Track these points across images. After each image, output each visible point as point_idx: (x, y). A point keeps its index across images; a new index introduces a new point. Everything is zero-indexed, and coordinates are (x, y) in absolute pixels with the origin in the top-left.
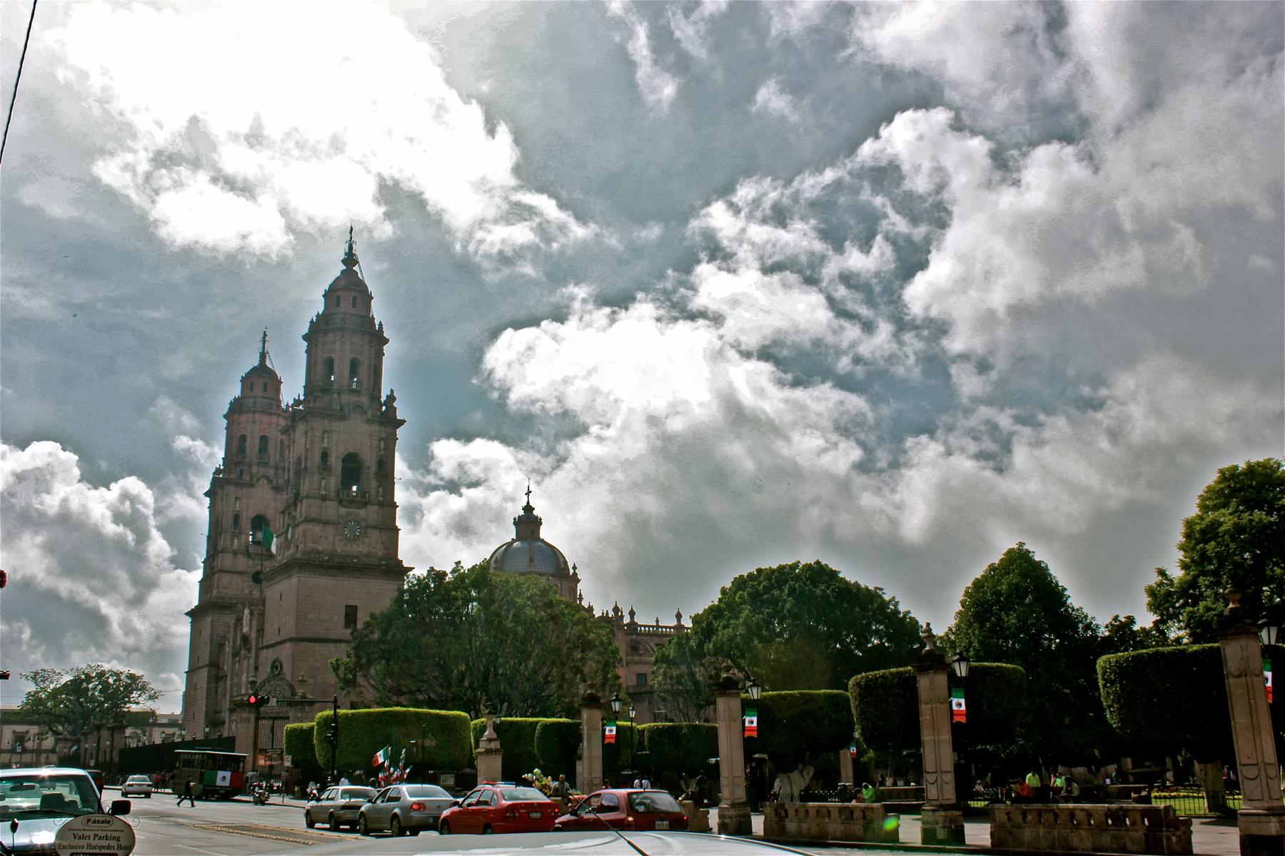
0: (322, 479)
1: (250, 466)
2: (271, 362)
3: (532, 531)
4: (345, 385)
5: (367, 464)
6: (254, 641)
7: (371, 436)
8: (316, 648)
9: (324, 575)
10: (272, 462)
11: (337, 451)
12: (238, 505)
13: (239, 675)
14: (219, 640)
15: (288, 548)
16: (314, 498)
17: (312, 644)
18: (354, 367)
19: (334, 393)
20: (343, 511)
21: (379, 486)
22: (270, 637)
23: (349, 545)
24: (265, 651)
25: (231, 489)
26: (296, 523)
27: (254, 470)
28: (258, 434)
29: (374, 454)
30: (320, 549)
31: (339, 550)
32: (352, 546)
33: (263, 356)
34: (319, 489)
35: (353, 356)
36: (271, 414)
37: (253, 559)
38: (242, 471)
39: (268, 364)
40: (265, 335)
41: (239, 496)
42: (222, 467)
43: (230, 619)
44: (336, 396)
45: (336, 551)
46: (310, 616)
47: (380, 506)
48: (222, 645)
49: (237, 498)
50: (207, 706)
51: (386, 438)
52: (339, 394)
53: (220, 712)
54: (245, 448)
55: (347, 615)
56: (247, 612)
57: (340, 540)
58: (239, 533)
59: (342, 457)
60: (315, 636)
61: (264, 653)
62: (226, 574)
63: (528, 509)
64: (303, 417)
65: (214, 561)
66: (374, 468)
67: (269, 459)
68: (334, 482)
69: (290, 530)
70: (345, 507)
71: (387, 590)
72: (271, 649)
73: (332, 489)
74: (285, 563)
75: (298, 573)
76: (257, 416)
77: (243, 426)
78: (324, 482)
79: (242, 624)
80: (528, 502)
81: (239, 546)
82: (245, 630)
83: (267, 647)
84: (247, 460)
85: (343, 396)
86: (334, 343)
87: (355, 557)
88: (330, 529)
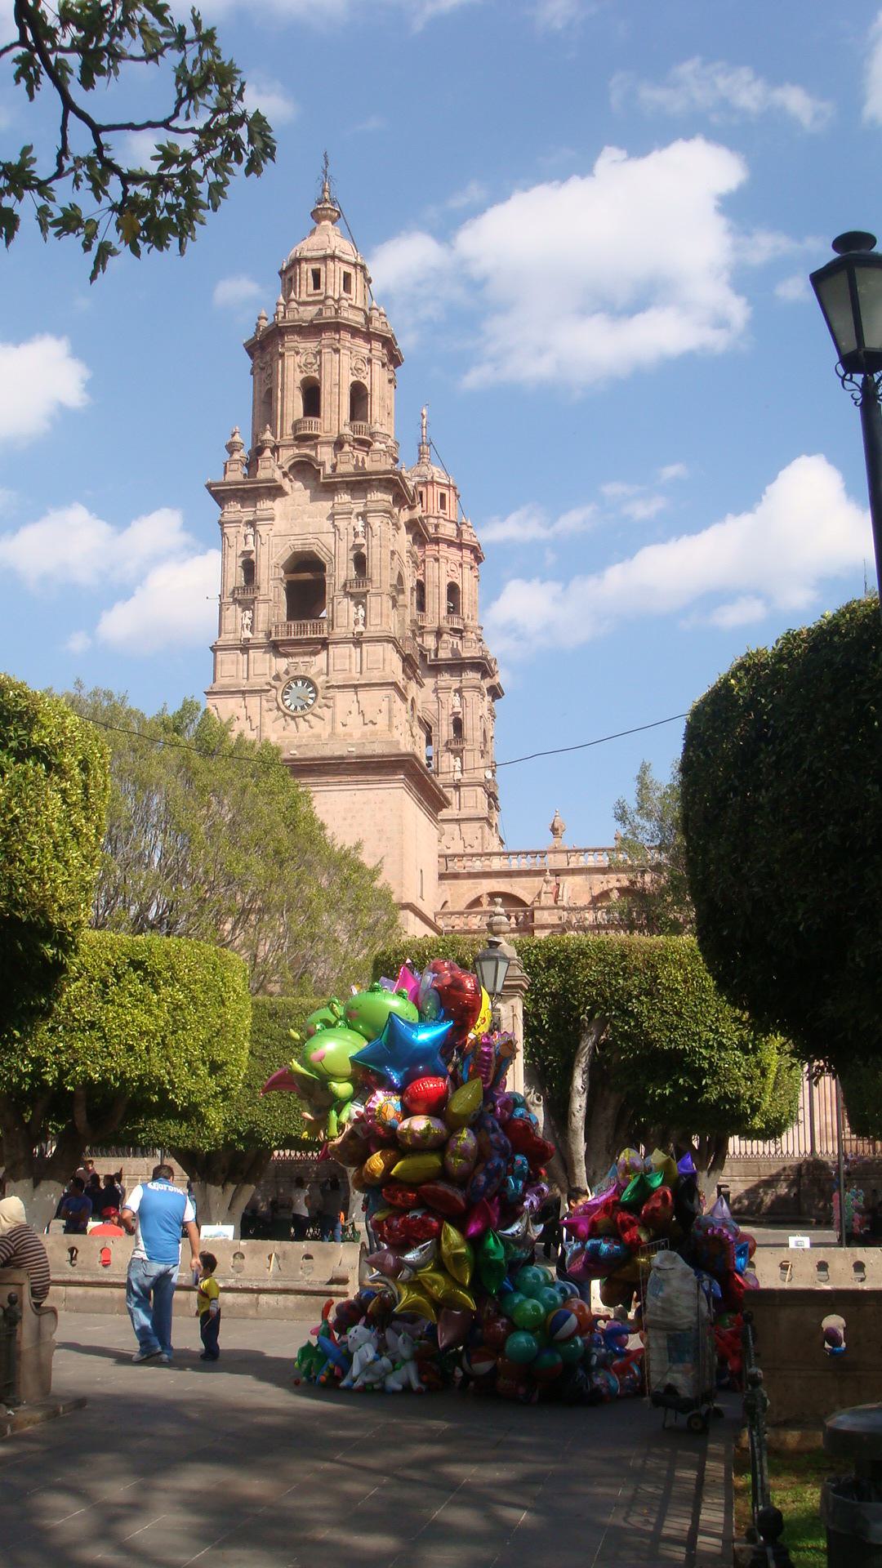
20: (282, 664)
35: (304, 375)
70: (286, 655)
88: (253, 701)
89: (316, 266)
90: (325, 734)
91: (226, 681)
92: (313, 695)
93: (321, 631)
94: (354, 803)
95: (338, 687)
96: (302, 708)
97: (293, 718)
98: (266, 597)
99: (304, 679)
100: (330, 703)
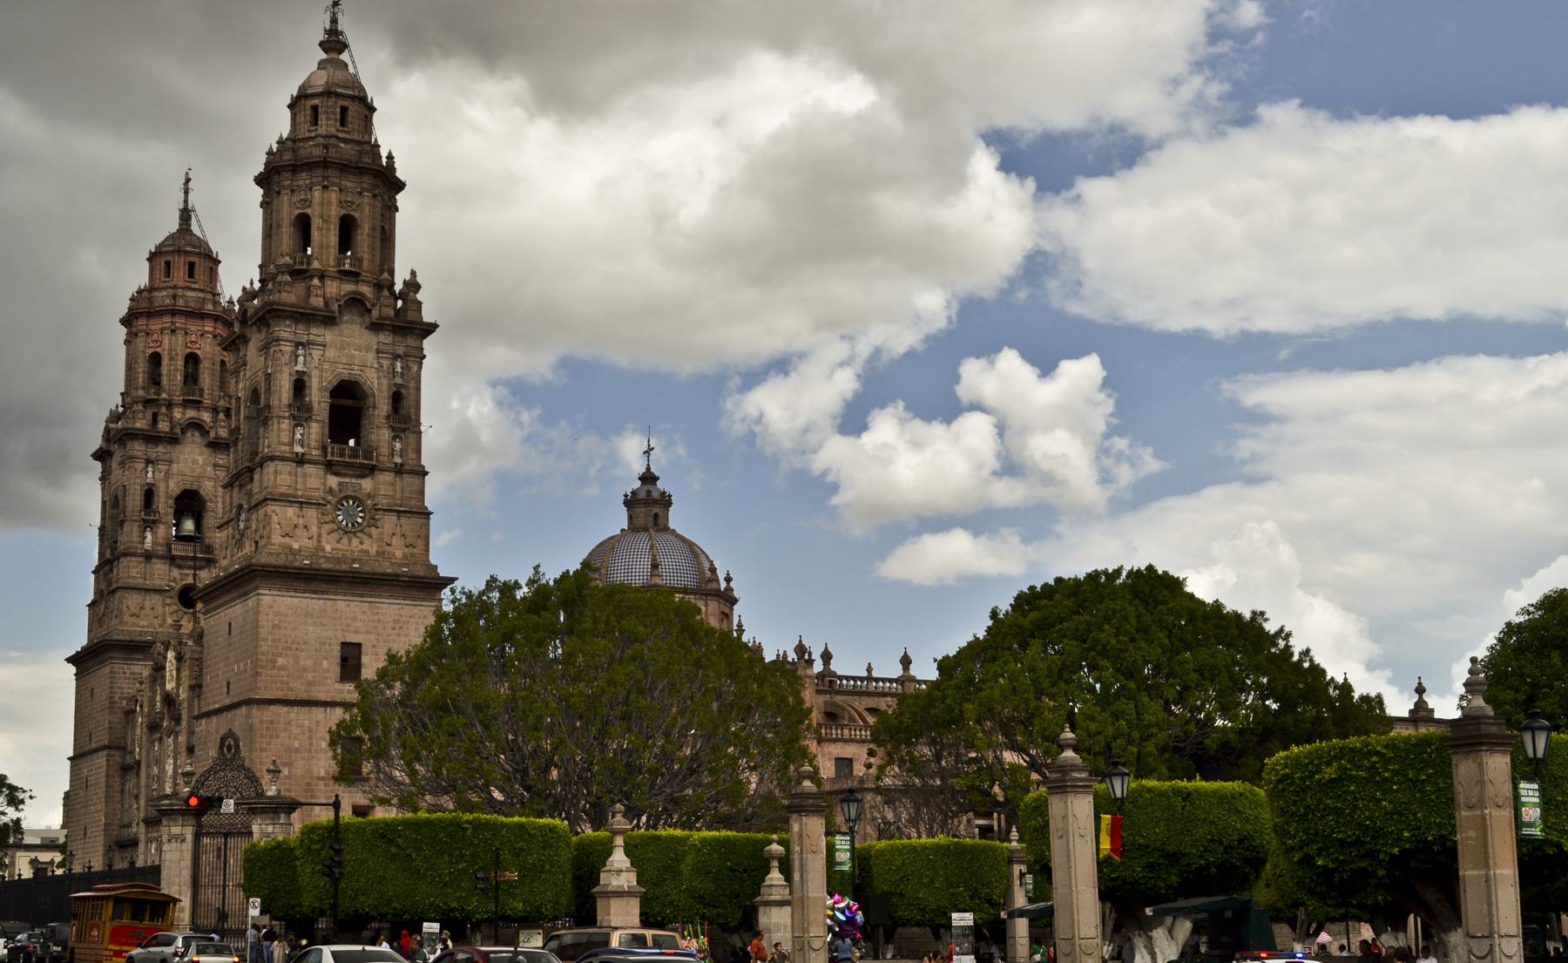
0: (296, 426)
1: (170, 405)
2: (200, 226)
3: (656, 515)
4: (332, 264)
6: (185, 705)
7: (378, 352)
8: (293, 716)
9: (304, 591)
10: (207, 401)
11: (321, 377)
12: (150, 475)
13: (160, 762)
14: (124, 702)
15: (239, 544)
16: (282, 459)
17: (285, 709)
18: (347, 228)
19: (312, 277)
20: (333, 481)
21: (394, 438)
22: (215, 697)
23: (345, 540)
24: (204, 721)
25: (137, 448)
26: (253, 503)
27: (177, 413)
28: (181, 352)
29: (385, 381)
30: (296, 546)
31: (328, 548)
33: (186, 214)
34: (291, 444)
35: (343, 212)
36: (201, 316)
37: (180, 567)
38: (155, 416)
39: (195, 228)
40: (188, 180)
41: (153, 456)
42: (121, 409)
43: (143, 669)
44: (316, 281)
45: (323, 550)
46: (280, 661)
47: (396, 472)
48: (130, 713)
50: (107, 816)
51: (406, 355)
52: (322, 277)
53: (129, 825)
54: (160, 375)
55: (344, 660)
56: (171, 655)
57: (332, 531)
58: (154, 522)
60: (291, 696)
61: (203, 725)
62: (134, 592)
63: (648, 478)
64: (259, 319)
65: (111, 571)
66: (383, 407)
67: (201, 396)
68: (316, 431)
69: (243, 516)
70: (336, 474)
72: (214, 719)
73: (313, 444)
74: (237, 571)
75: (257, 588)
76: (180, 321)
77: (155, 337)
78: (299, 431)
79: (163, 677)
80: (648, 468)
82: (169, 686)
83: (209, 714)
84: (164, 396)
85: (328, 282)
86: (311, 189)
87: (354, 561)
88: (312, 513)
89: (346, 103)
90: (373, 551)
91: (283, 490)
92: (361, 515)
93: (371, 459)
94: (401, 616)
95: (385, 510)
96: (353, 524)
97: (346, 532)
98: (318, 418)
99: (355, 499)
100: (379, 523)
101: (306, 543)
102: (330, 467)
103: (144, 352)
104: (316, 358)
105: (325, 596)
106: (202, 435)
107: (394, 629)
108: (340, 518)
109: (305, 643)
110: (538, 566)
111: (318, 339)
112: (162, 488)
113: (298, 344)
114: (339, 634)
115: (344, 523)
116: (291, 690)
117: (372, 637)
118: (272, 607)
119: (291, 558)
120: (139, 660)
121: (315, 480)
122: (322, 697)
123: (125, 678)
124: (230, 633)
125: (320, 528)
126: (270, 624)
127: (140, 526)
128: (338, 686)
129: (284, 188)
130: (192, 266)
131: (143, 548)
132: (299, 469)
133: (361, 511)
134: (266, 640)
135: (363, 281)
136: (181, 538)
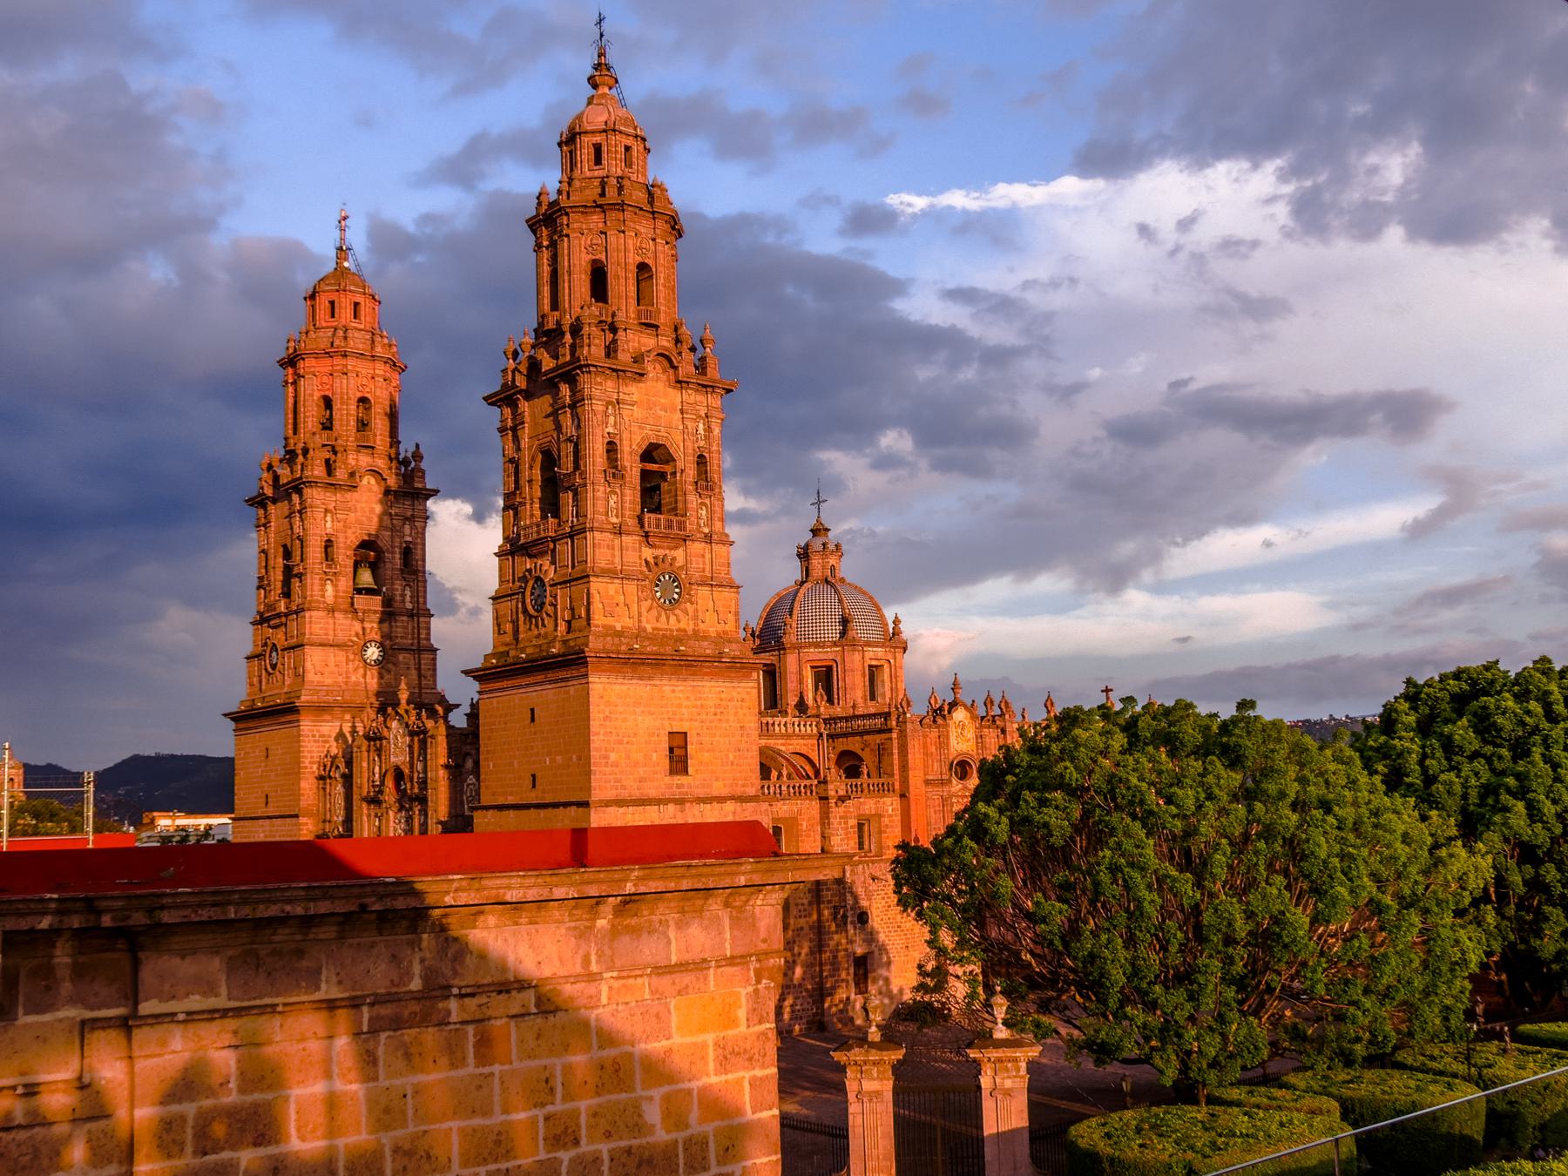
5: (680, 465)
7: (682, 412)
12: (329, 525)
14: (315, 766)
20: (648, 553)
23: (663, 617)
27: (352, 459)
31: (649, 628)
32: (668, 618)
35: (639, 259)
41: (331, 507)
46: (613, 756)
49: (326, 511)
55: (671, 750)
59: (640, 451)
60: (625, 794)
66: (691, 473)
67: (375, 442)
68: (631, 495)
71: (731, 700)
76: (351, 363)
81: (336, 597)
88: (632, 587)
89: (630, 142)
92: (677, 590)
96: (670, 602)
97: (665, 610)
101: (629, 623)
102: (647, 535)
103: (312, 395)
104: (626, 419)
105: (651, 682)
106: (378, 483)
107: (715, 714)
108: (658, 594)
109: (635, 735)
110: (1111, 690)
111: (627, 397)
112: (341, 540)
113: (609, 403)
114: (666, 723)
115: (662, 600)
116: (624, 787)
117: (697, 724)
118: (602, 697)
119: (617, 640)
120: (328, 721)
121: (635, 553)
122: (653, 793)
123: (315, 741)
124: (533, 720)
125: (639, 606)
126: (602, 716)
127: (321, 579)
128: (668, 779)
129: (574, 230)
130: (356, 304)
131: (324, 602)
132: (617, 542)
133: (676, 587)
134: (598, 734)
135: (662, 335)
136: (359, 591)
